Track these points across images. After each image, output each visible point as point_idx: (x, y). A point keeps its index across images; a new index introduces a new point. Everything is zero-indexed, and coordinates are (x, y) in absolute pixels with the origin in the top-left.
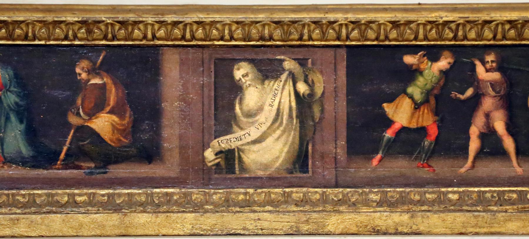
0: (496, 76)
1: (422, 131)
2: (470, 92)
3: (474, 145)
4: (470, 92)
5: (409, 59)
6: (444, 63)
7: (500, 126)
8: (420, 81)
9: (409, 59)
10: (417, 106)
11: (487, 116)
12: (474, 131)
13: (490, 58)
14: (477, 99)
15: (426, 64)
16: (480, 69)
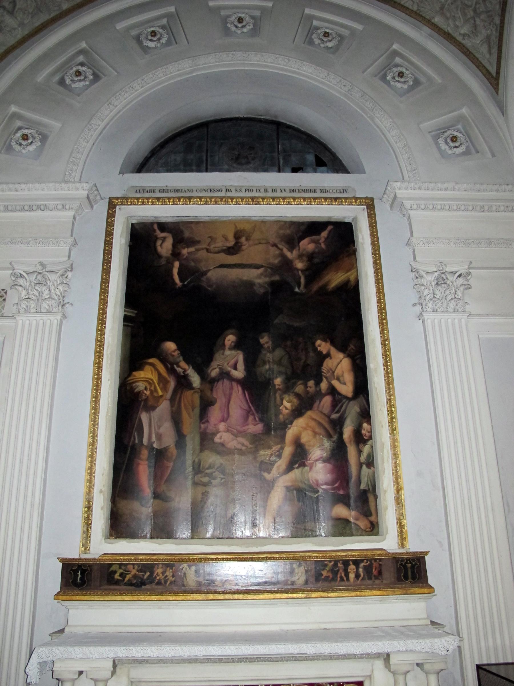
0: (342, 565)
1: (328, 577)
2: (337, 569)
3: (339, 579)
4: (337, 569)
5: (326, 562)
6: (332, 563)
7: (343, 575)
8: (328, 567)
9: (326, 562)
10: (328, 571)
11: (341, 573)
12: (339, 576)
13: (341, 562)
14: (338, 570)
15: (329, 563)
16: (339, 564)
